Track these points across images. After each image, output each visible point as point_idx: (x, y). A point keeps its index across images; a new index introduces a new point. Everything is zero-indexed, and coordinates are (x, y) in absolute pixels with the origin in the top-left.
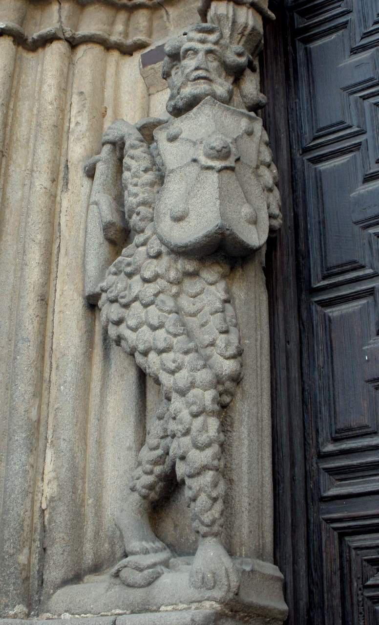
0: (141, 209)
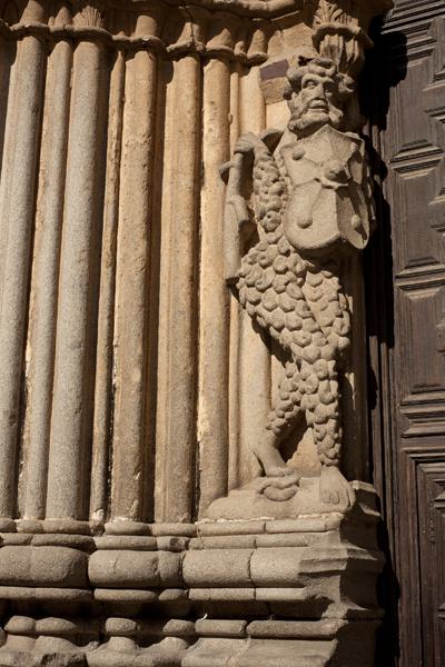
0: (272, 213)
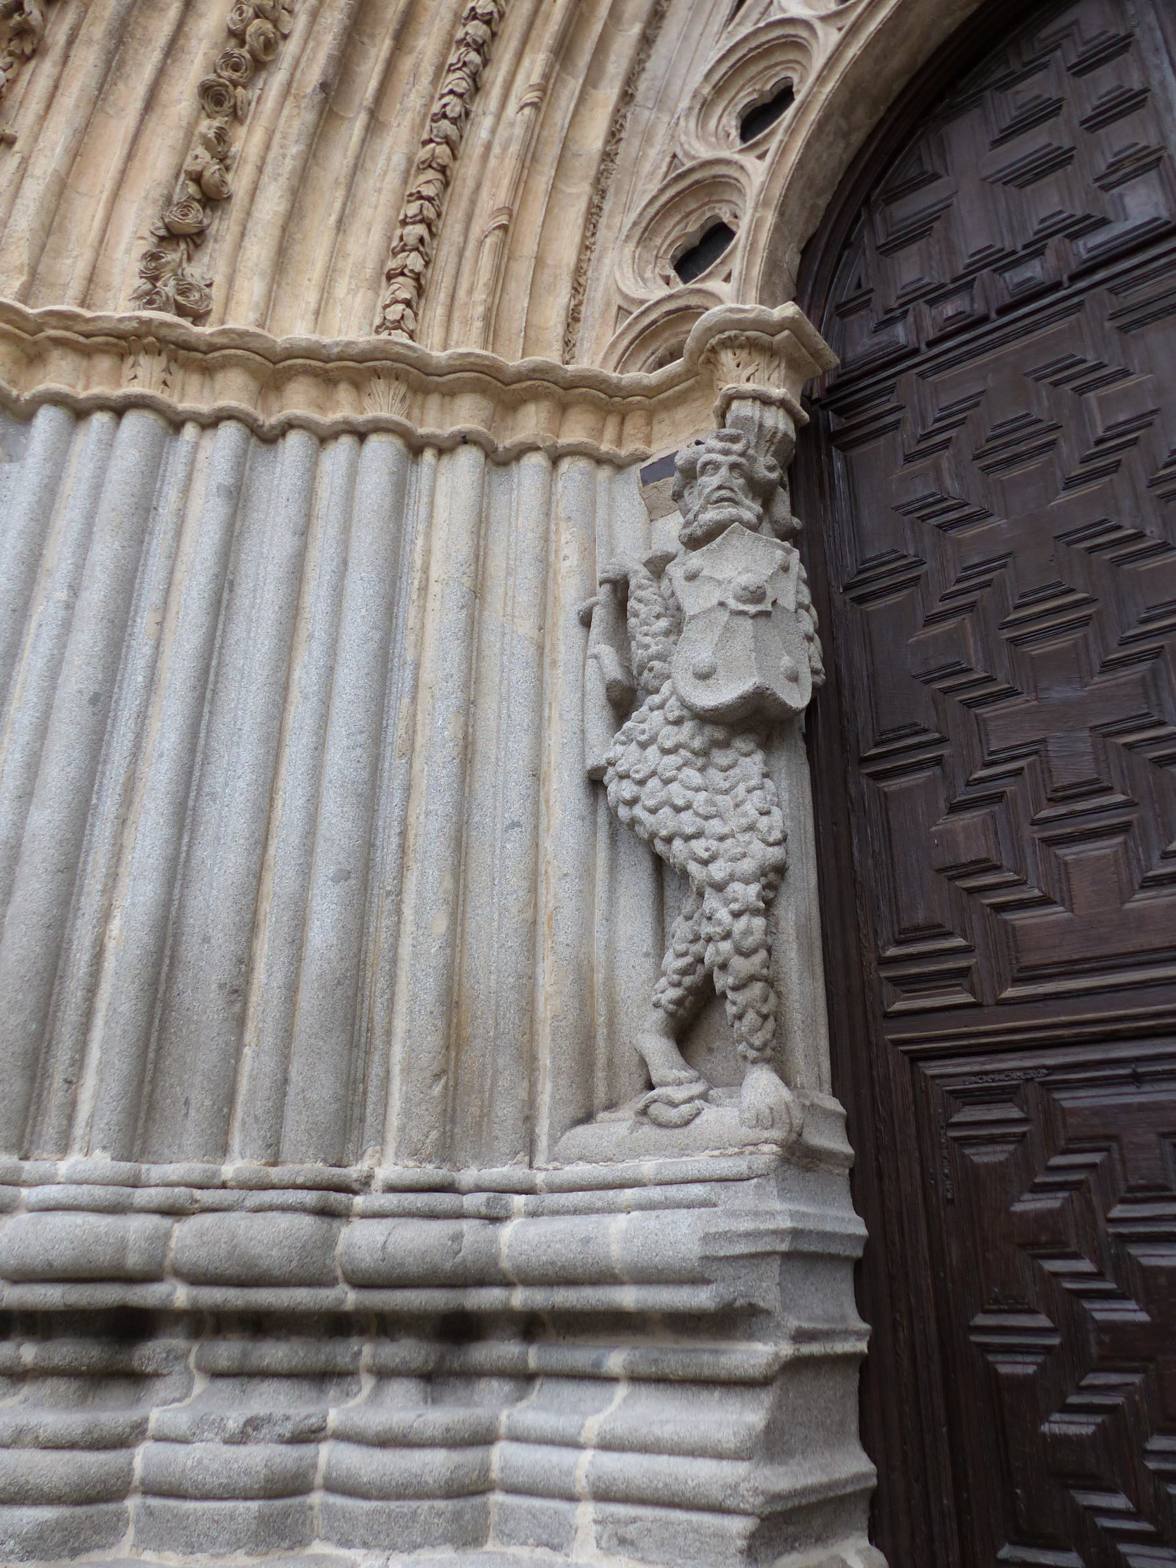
0: (656, 664)
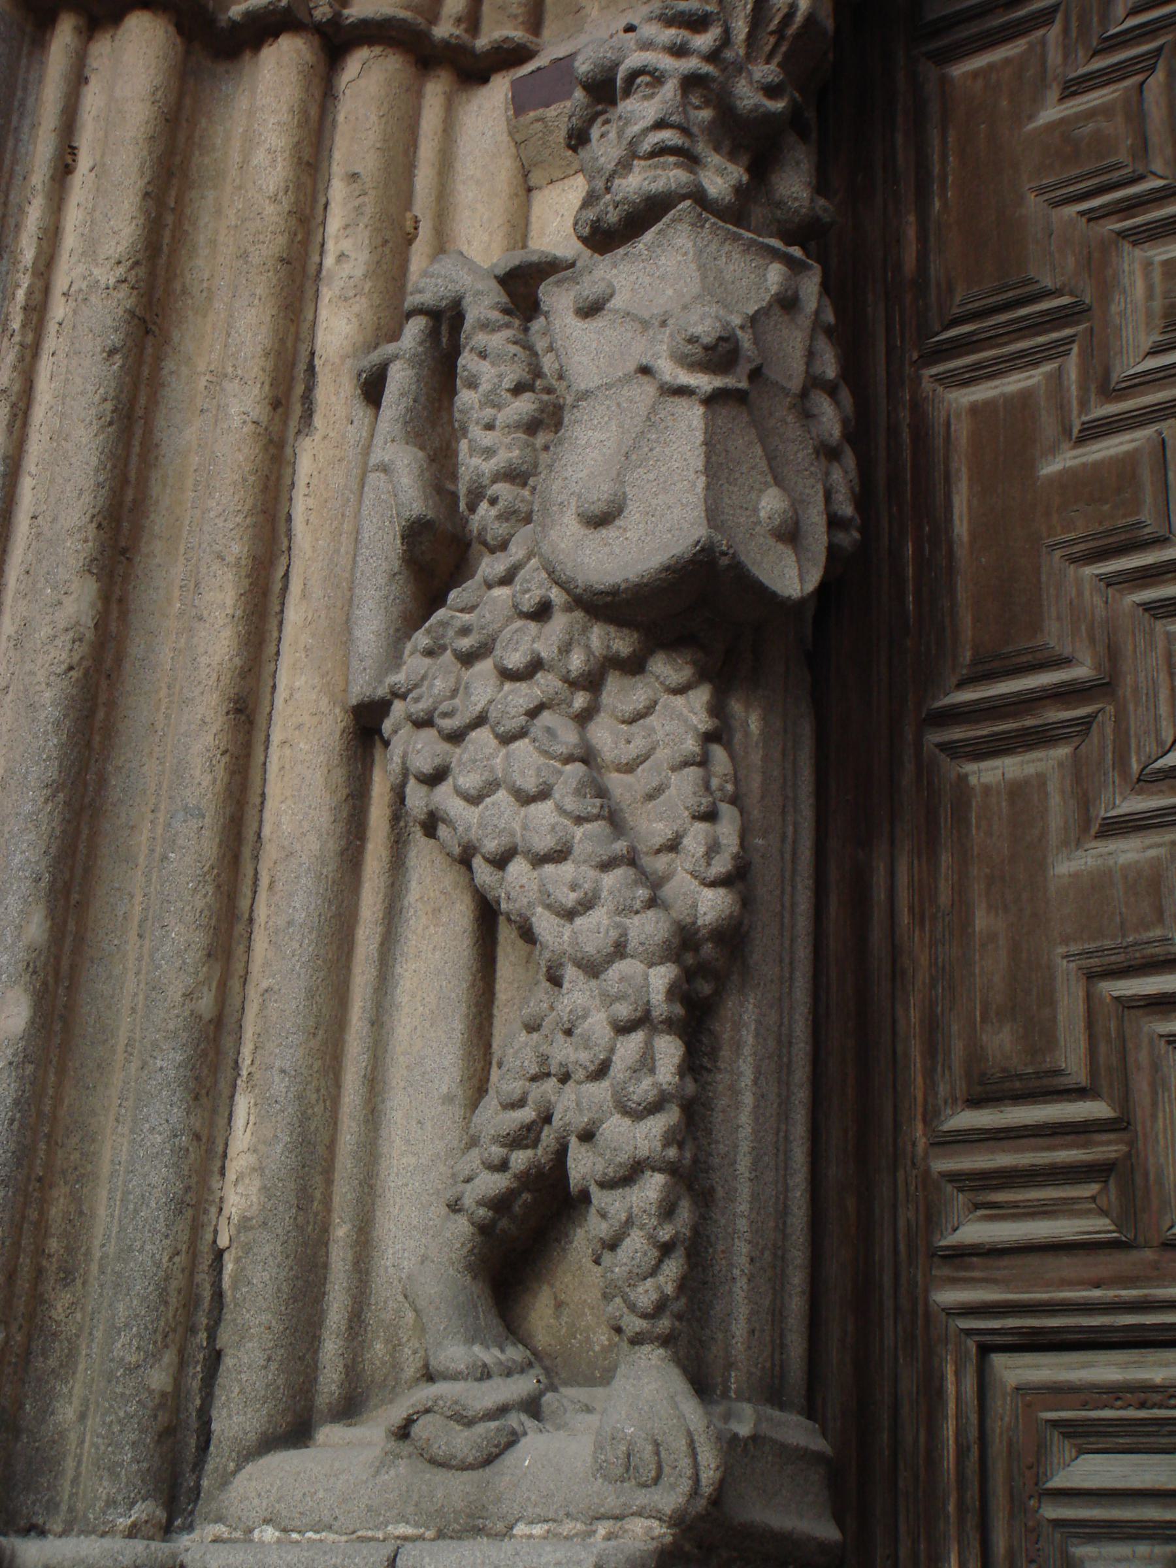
0: (502, 489)
